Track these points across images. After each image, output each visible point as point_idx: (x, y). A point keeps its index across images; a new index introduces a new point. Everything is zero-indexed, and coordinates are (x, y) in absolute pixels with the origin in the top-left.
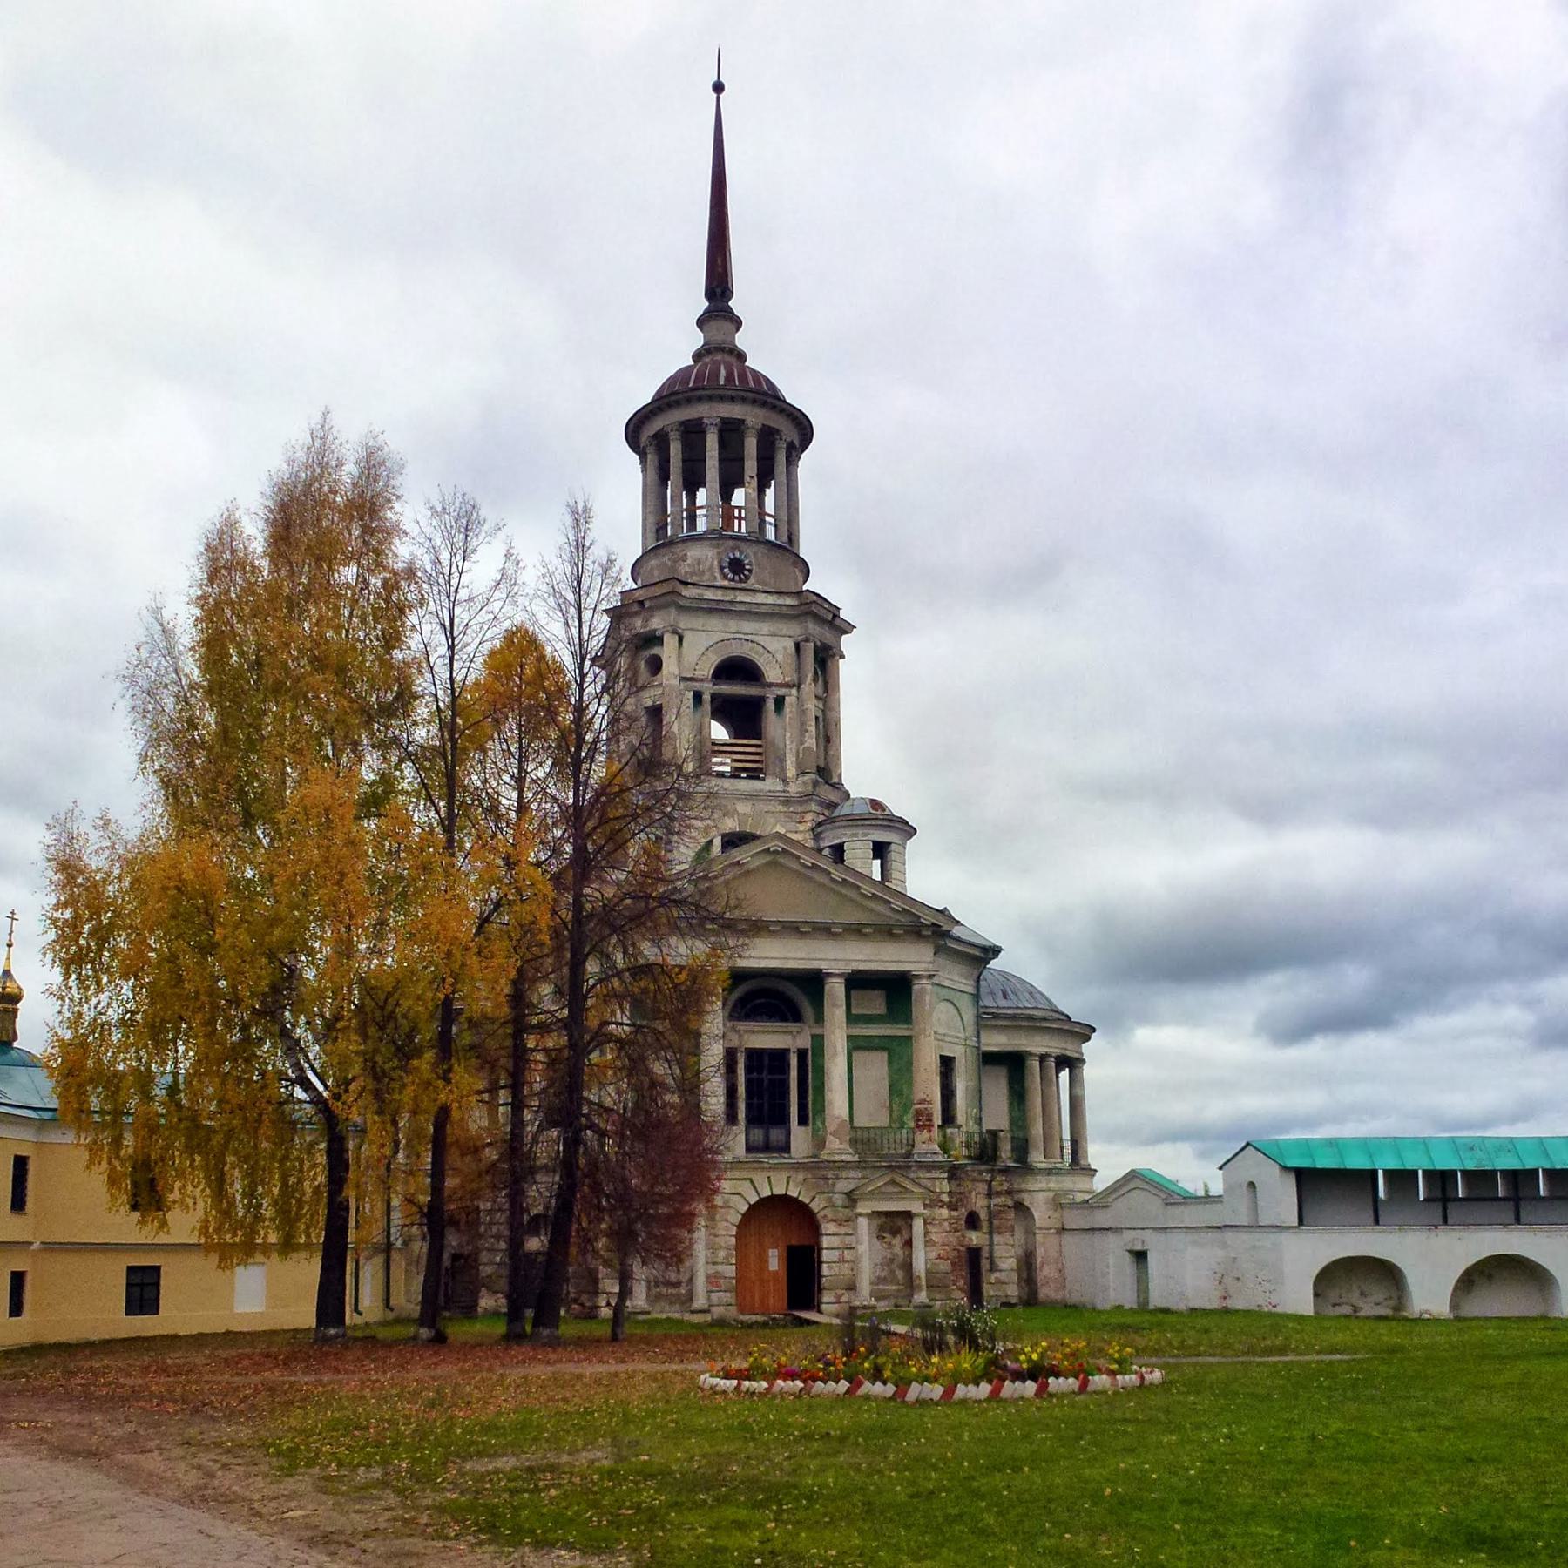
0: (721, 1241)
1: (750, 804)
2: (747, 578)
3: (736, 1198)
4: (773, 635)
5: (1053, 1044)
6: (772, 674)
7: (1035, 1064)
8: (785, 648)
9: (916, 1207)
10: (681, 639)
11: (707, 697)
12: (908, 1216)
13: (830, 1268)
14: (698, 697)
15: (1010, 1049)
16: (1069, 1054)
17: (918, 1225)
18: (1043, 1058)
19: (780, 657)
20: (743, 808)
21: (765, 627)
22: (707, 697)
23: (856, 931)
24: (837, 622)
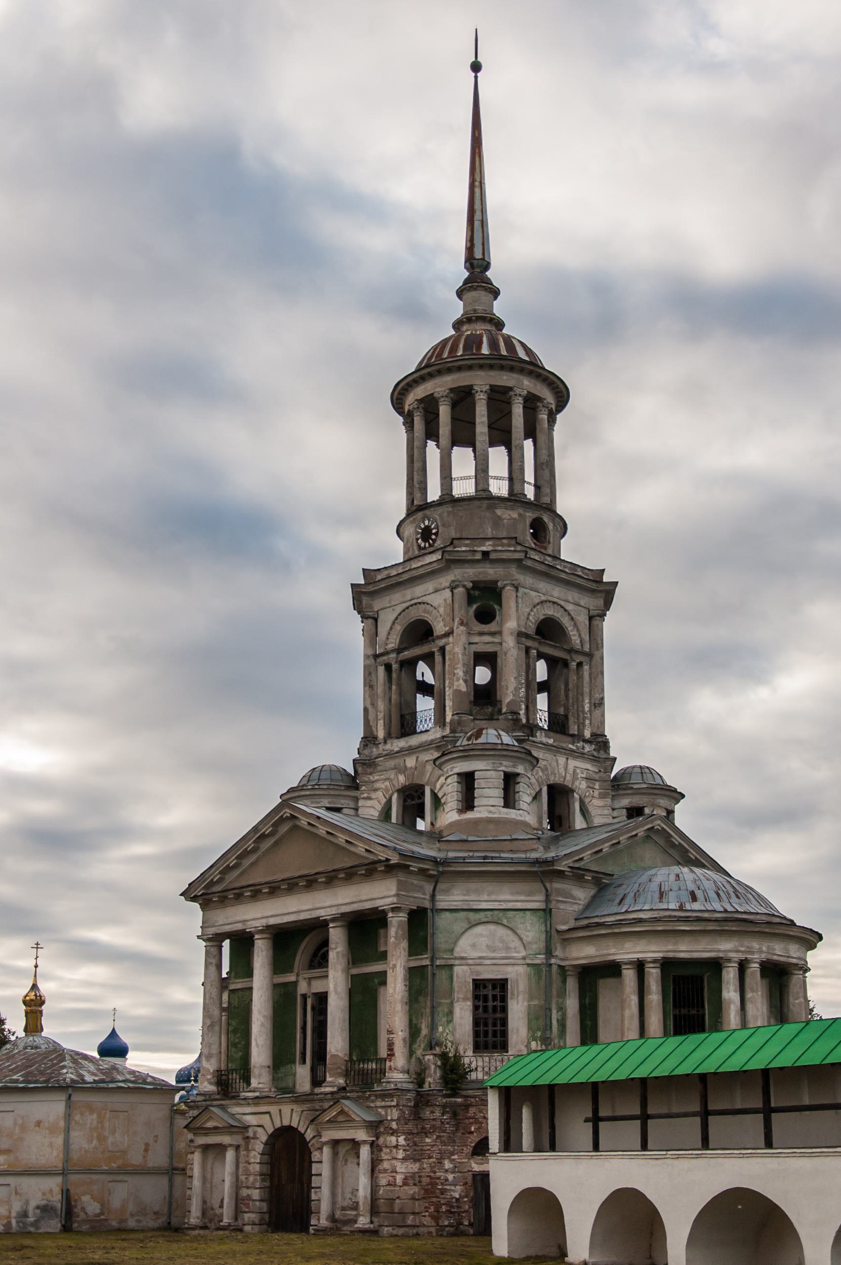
0: (251, 1167)
1: (414, 758)
2: (434, 541)
3: (260, 1130)
4: (436, 591)
5: (653, 948)
6: (439, 628)
7: (629, 975)
8: (445, 600)
9: (361, 1135)
10: (376, 620)
11: (395, 666)
12: (355, 1145)
13: (316, 1193)
14: (388, 667)
15: (597, 960)
16: (682, 955)
17: (365, 1151)
18: (640, 966)
19: (442, 610)
20: (411, 762)
21: (429, 586)
22: (395, 666)
23: (332, 879)
24: (493, 556)
